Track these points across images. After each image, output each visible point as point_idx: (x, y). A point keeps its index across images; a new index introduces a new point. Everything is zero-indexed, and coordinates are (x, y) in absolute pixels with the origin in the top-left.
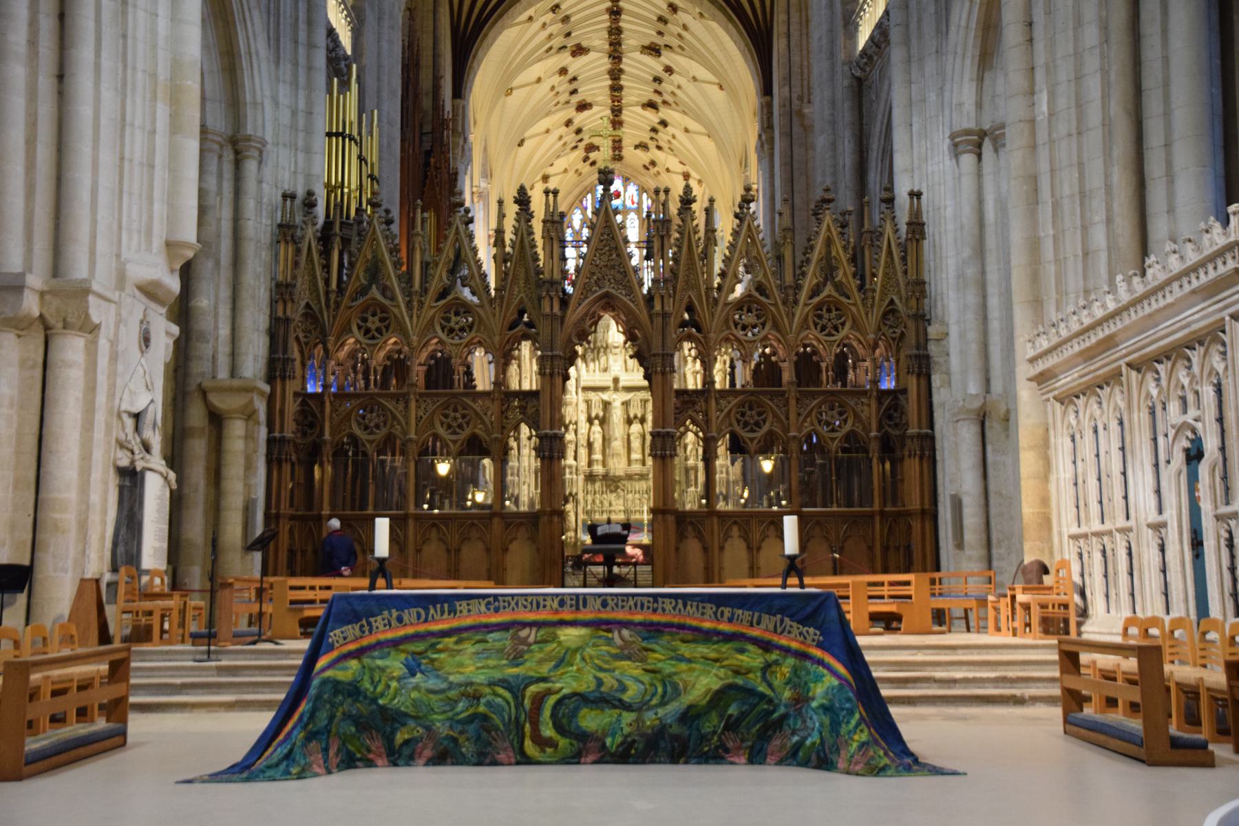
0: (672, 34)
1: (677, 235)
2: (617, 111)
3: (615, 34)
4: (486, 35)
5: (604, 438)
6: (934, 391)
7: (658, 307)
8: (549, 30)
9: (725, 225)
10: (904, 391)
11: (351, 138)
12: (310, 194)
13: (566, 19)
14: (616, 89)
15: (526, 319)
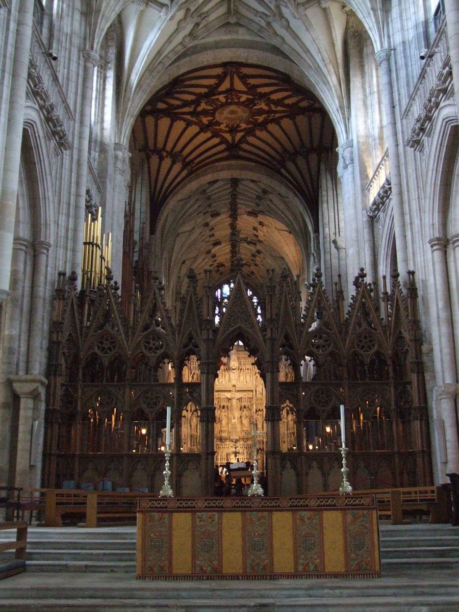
6: (426, 382)
11: (97, 246)
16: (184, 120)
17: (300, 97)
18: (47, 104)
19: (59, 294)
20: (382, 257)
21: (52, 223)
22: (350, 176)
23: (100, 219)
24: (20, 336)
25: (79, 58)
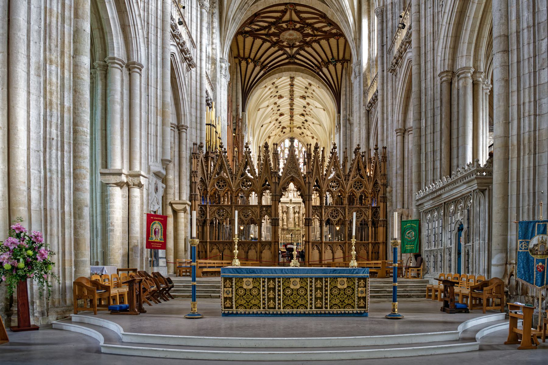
0: (309, 93)
1: (313, 158)
2: (292, 116)
3: (292, 92)
4: (252, 92)
5: (287, 218)
7: (307, 181)
9: (328, 155)
12: (201, 143)
13: (276, 87)
14: (292, 109)
15: (267, 183)
16: (262, 38)
17: (332, 27)
18: (181, 41)
19: (194, 155)
20: (372, 135)
21: (188, 114)
22: (358, 84)
23: (214, 109)
24: (174, 178)
25: (197, 6)
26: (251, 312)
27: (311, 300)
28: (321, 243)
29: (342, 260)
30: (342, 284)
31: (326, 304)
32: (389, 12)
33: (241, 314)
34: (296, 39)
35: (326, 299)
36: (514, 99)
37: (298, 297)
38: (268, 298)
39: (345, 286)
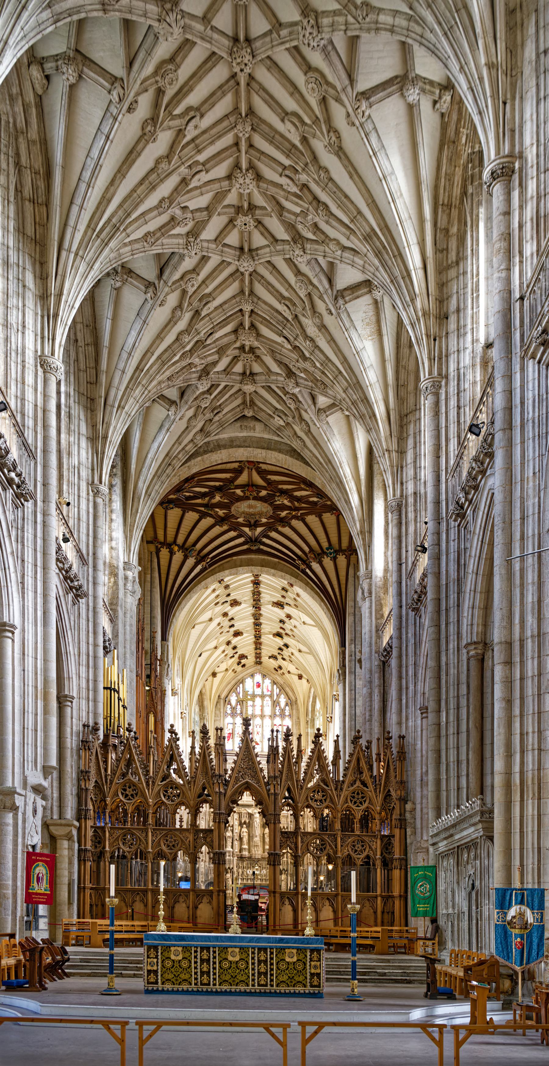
1: (281, 759)
8: (217, 593)
9: (308, 748)
10: (393, 836)
13: (227, 587)
16: (198, 511)
26: (180, 989)
27: (253, 975)
28: (297, 894)
29: (331, 924)
30: (291, 957)
31: (272, 980)
32: (411, 509)
33: (168, 991)
34: (261, 514)
35: (272, 975)
36: (517, 725)
37: (238, 971)
38: (201, 971)
39: (295, 959)
